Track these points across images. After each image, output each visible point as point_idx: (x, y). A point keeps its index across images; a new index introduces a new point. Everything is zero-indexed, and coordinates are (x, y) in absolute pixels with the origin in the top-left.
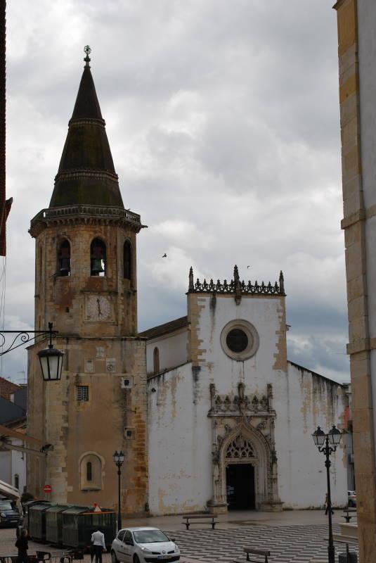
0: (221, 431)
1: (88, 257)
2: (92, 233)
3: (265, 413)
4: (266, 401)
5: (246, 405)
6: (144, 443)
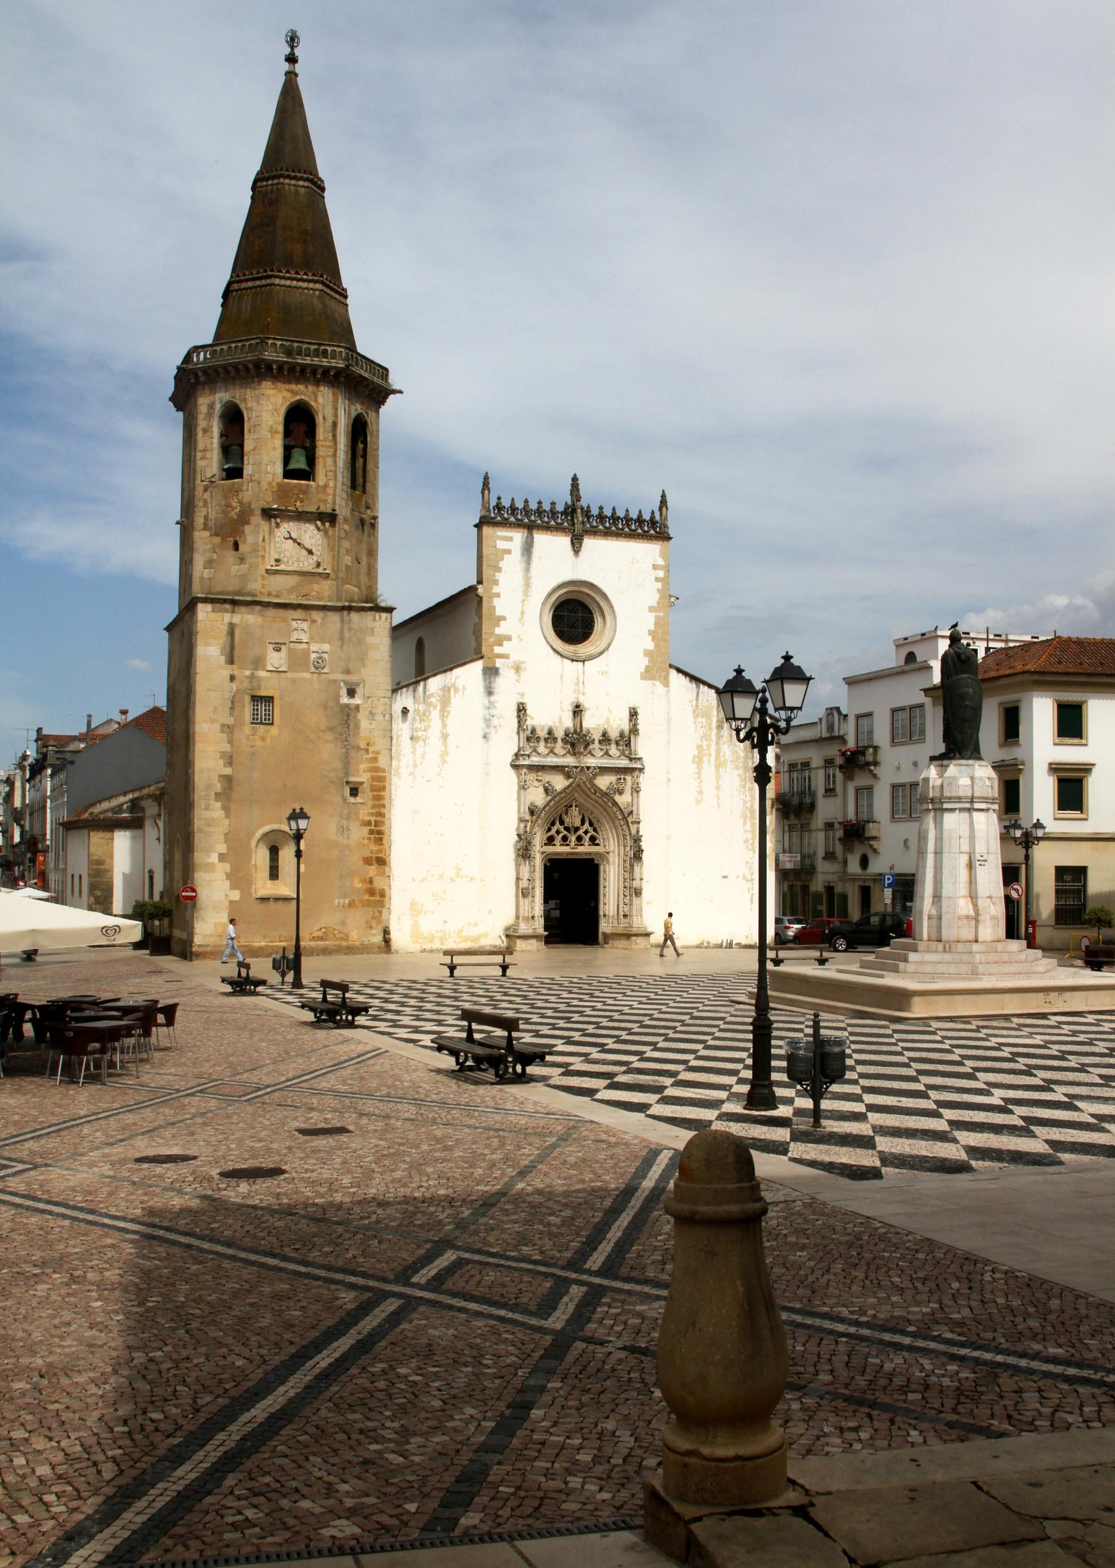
0: (537, 796)
1: (278, 442)
2: (288, 395)
3: (624, 763)
4: (626, 741)
6: (382, 810)
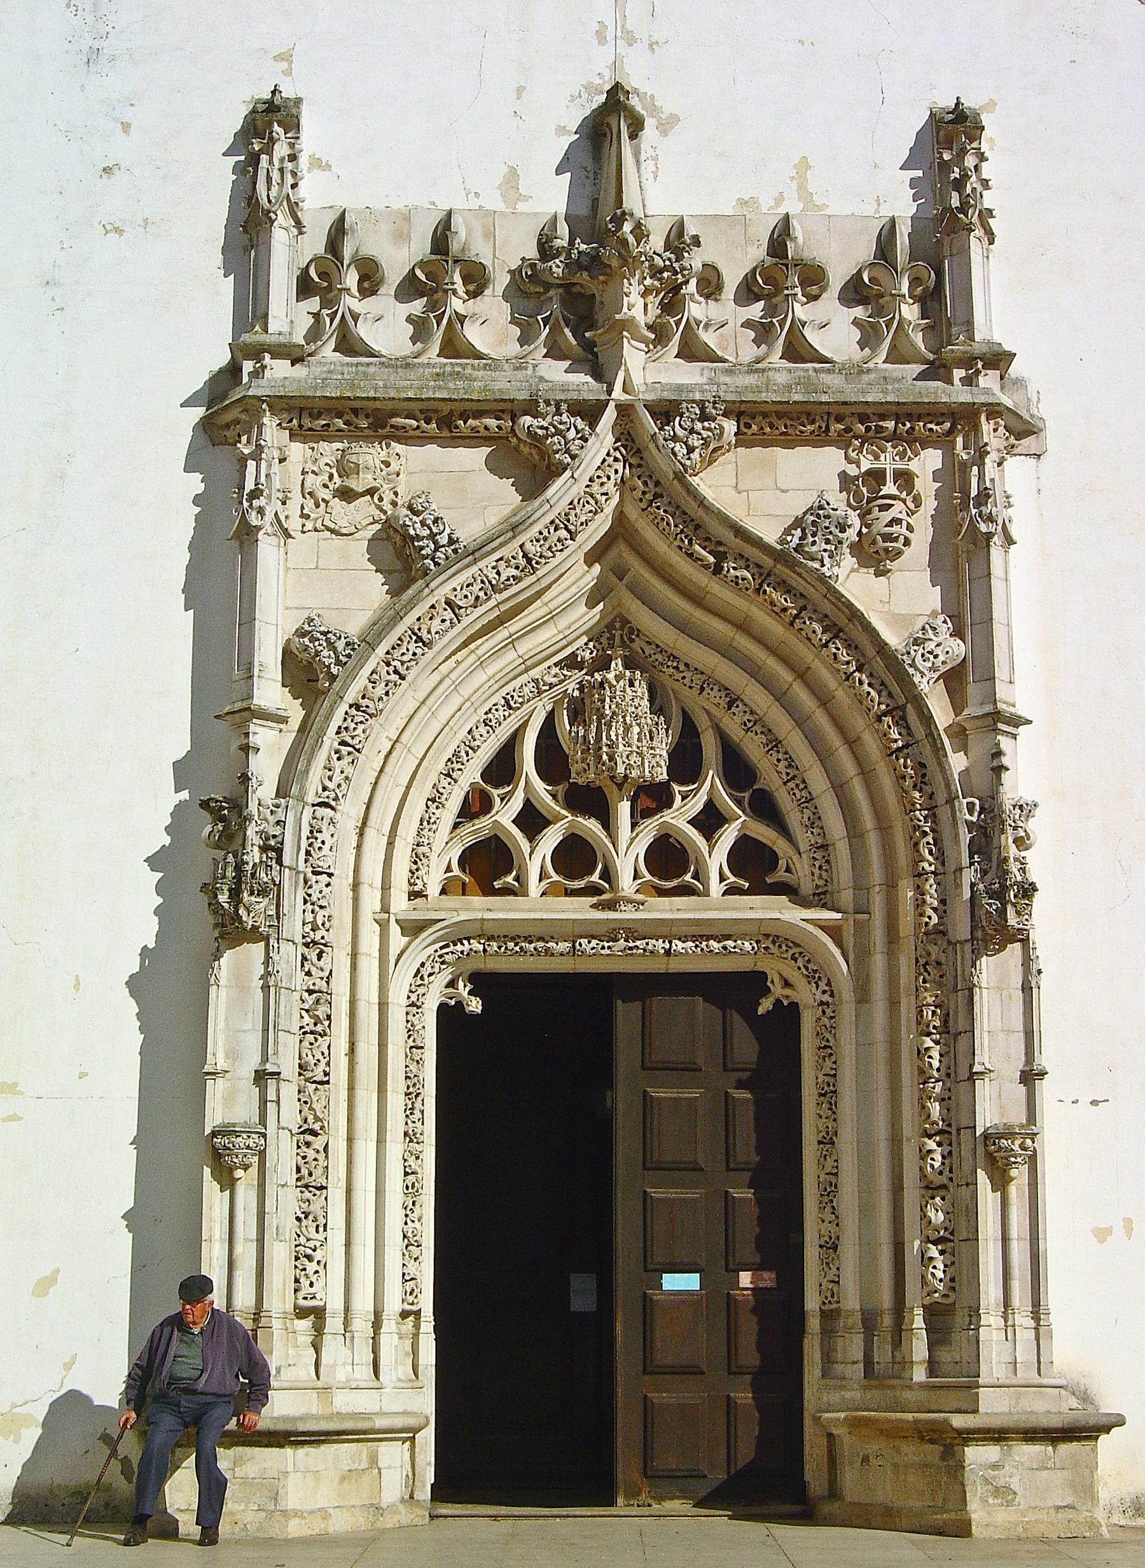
5: (672, 302)
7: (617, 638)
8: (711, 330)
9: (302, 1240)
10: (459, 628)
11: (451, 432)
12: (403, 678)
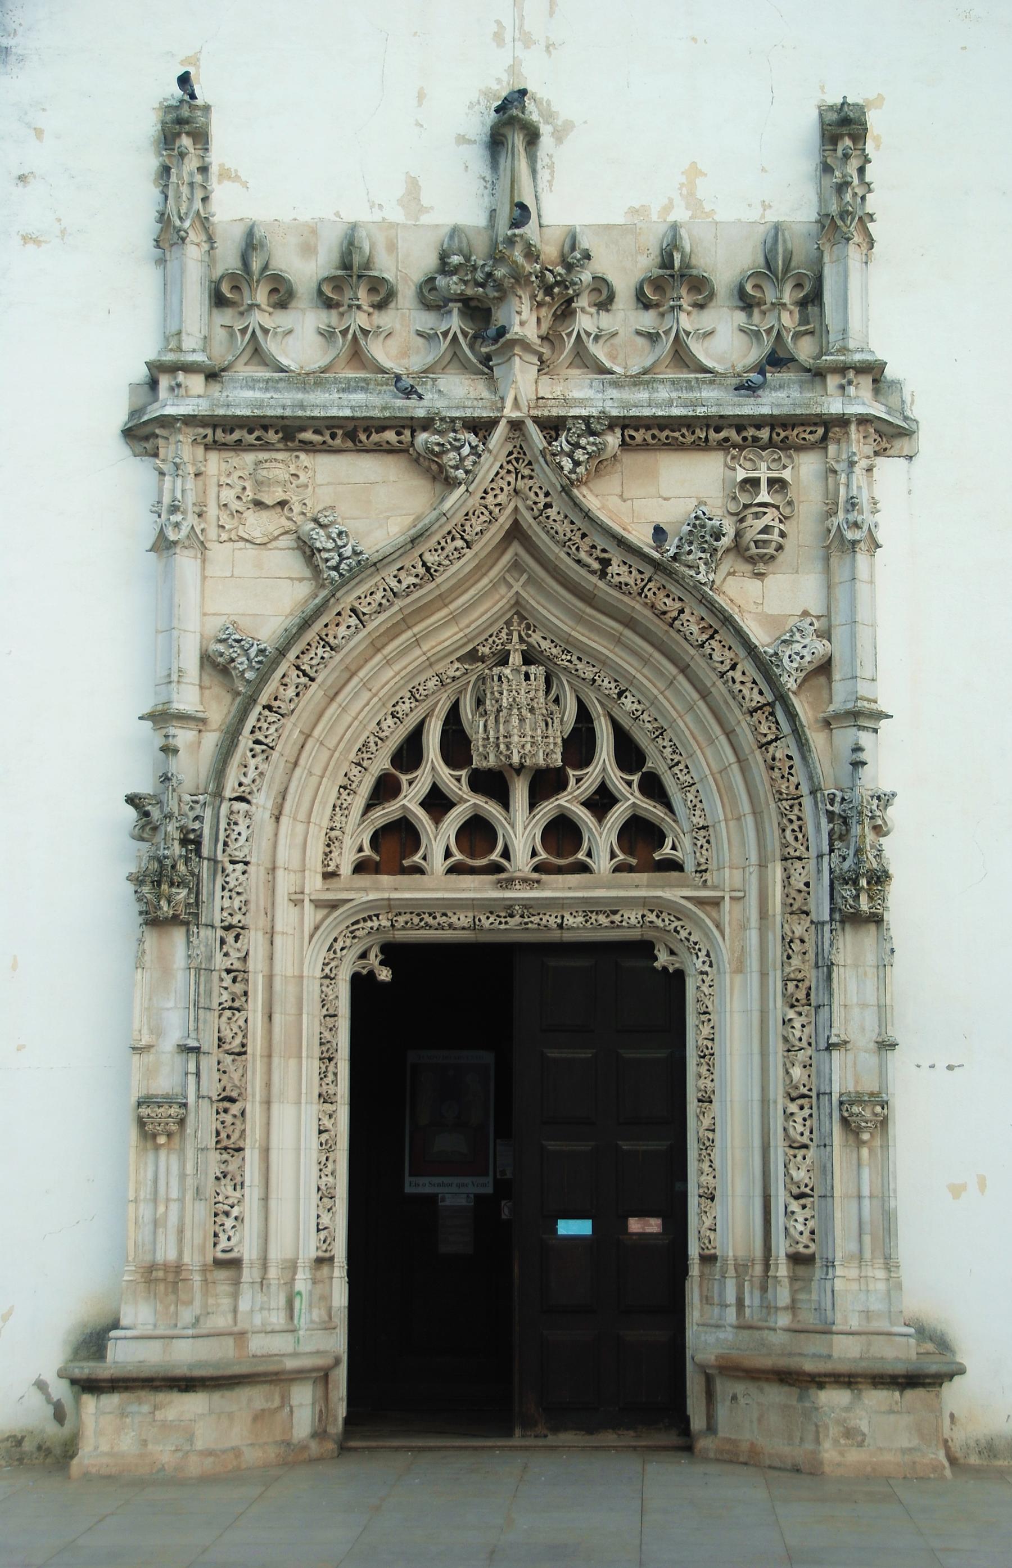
0: (259, 593)
7: (515, 635)
8: (601, 341)
9: (220, 1198)
10: (364, 632)
11: (355, 445)
12: (312, 680)
